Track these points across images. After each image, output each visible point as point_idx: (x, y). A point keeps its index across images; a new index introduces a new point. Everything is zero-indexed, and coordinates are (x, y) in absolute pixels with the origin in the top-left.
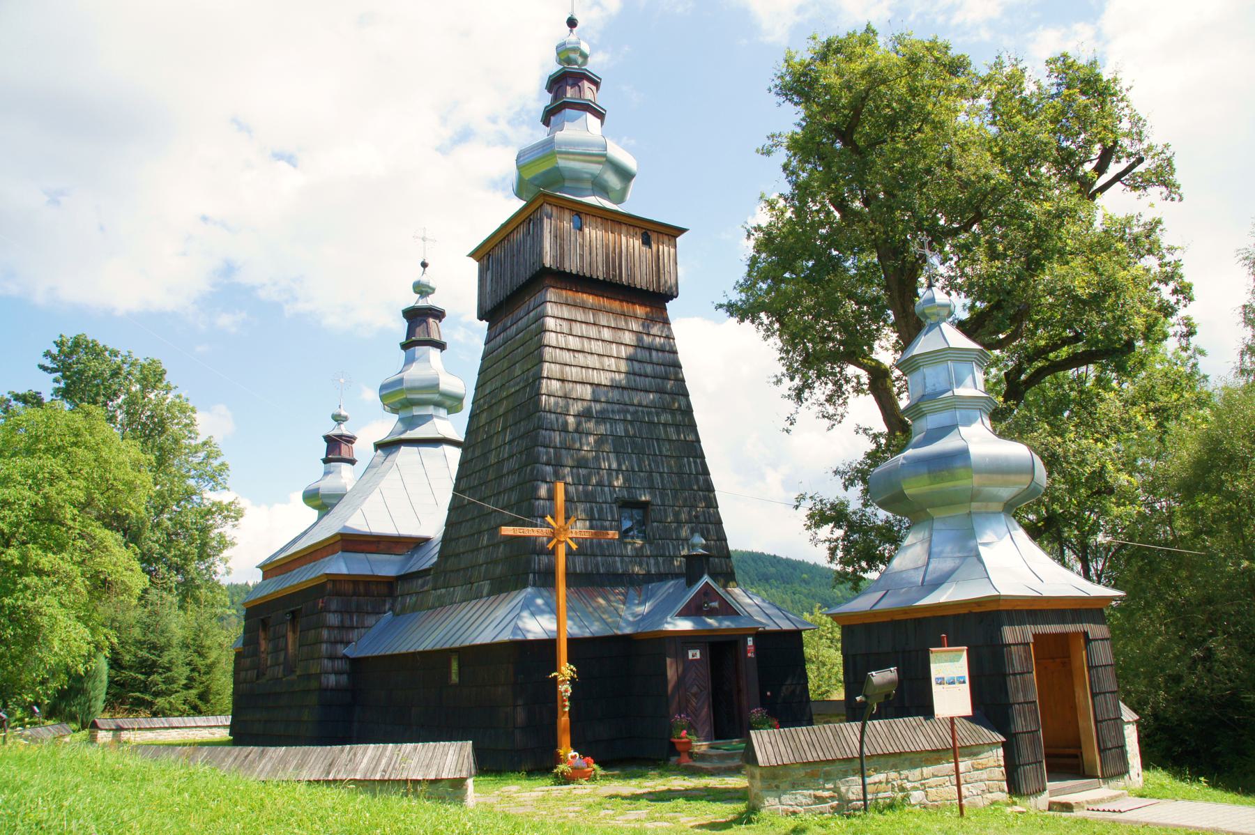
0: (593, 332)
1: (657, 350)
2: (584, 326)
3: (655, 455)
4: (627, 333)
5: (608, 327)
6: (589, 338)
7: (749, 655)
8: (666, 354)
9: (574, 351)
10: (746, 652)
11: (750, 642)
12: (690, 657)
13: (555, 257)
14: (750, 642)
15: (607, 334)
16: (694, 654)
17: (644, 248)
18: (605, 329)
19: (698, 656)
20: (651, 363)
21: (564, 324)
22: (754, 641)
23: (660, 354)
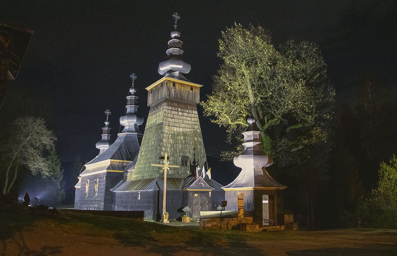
0: (176, 113)
1: (193, 118)
2: (174, 111)
3: (191, 145)
4: (185, 113)
5: (181, 112)
6: (176, 115)
7: (210, 196)
8: (196, 119)
9: (172, 118)
10: (209, 195)
11: (210, 193)
12: (195, 196)
13: (171, 173)
14: (210, 193)
15: (180, 113)
16: (196, 195)
17: (191, 91)
18: (180, 112)
19: (197, 196)
20: (191, 121)
21: (170, 111)
22: (211, 193)
23: (194, 118)
